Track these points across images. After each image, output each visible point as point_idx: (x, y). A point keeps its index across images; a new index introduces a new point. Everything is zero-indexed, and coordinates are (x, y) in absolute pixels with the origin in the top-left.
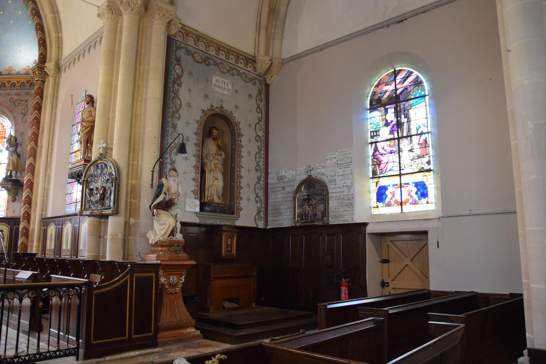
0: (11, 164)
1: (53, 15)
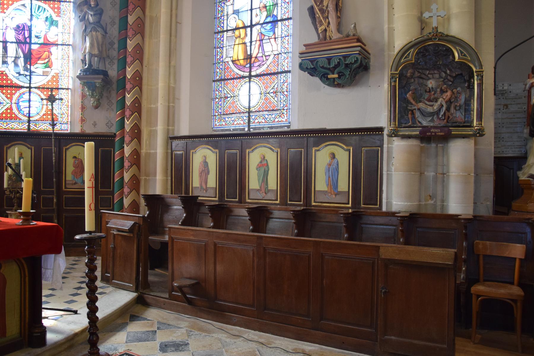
0: (96, 45)
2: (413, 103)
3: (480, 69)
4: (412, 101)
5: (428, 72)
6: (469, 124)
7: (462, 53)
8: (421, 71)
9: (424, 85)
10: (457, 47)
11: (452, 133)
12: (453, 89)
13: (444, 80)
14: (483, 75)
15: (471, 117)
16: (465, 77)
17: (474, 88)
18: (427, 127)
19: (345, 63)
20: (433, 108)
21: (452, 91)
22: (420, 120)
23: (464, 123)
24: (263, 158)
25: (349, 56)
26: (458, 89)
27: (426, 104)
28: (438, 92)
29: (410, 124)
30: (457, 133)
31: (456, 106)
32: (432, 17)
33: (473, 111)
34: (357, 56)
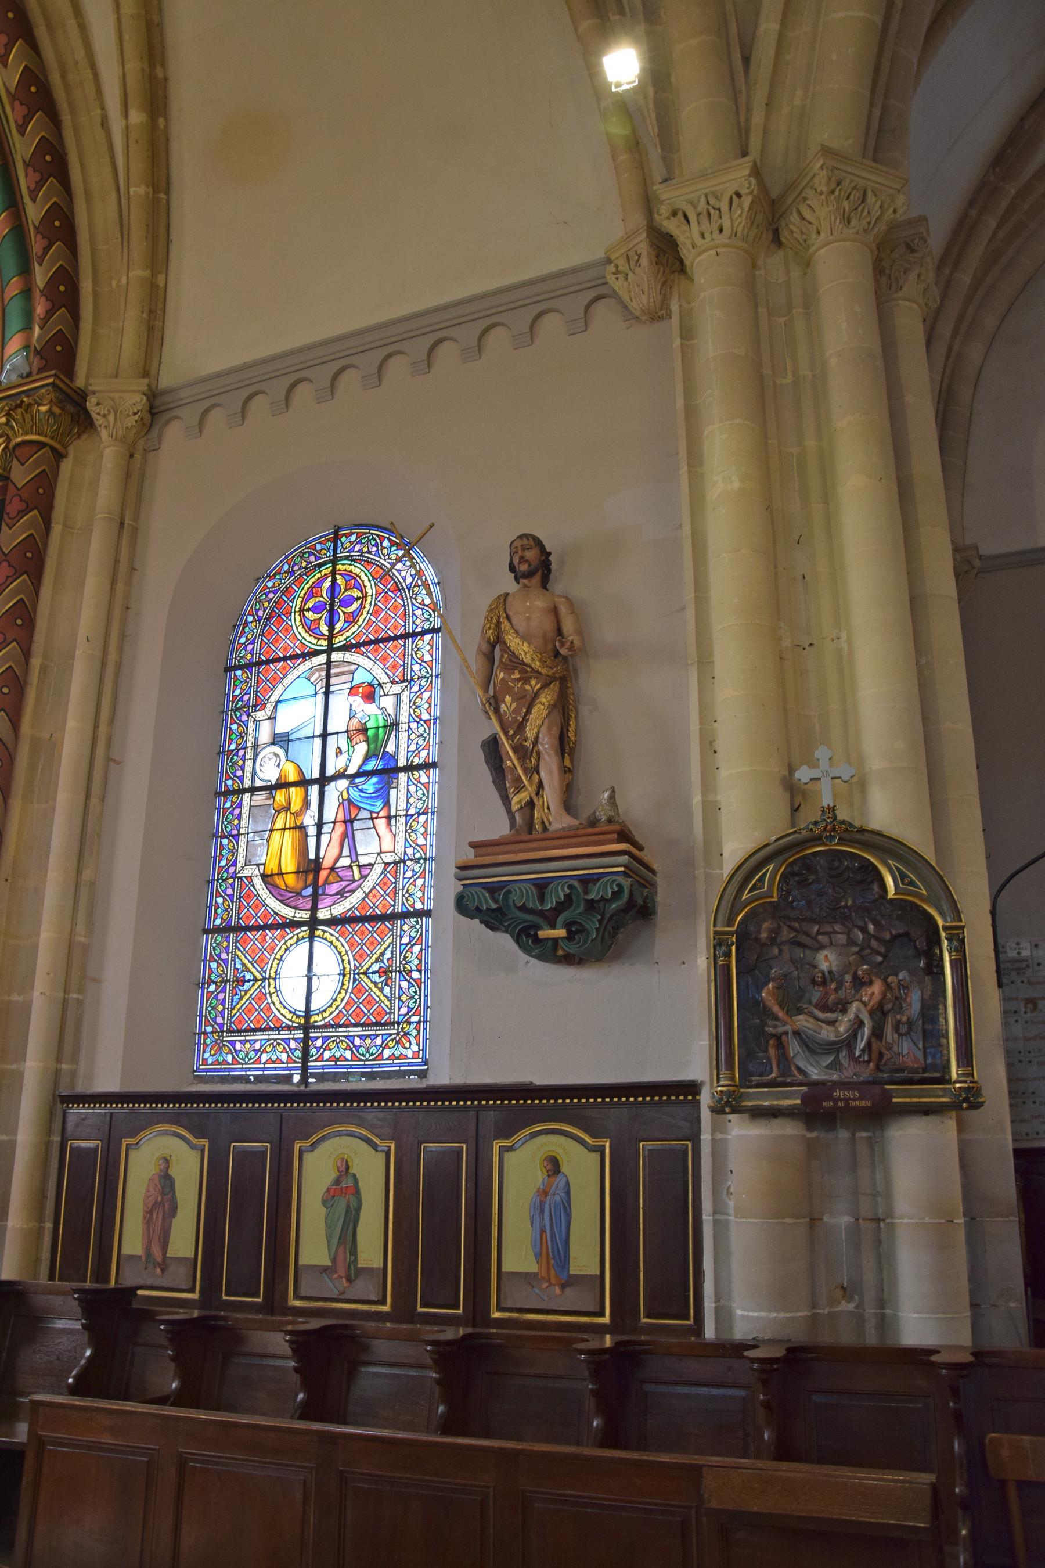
1: (151, 190)
2: (781, 1014)
3: (953, 920)
4: (776, 1009)
5: (816, 928)
6: (938, 1075)
7: (903, 876)
8: (797, 925)
9: (807, 963)
10: (890, 862)
11: (894, 1100)
12: (889, 976)
13: (860, 951)
14: (964, 938)
15: (942, 1055)
16: (917, 943)
17: (943, 973)
18: (822, 1083)
19: (586, 897)
20: (837, 1031)
21: (885, 980)
22: (801, 1064)
23: (925, 1071)
24: (345, 1170)
25: (598, 880)
26: (901, 977)
27: (817, 1019)
28: (848, 984)
29: (774, 1075)
30: (908, 1100)
31: (899, 1022)
32: (819, 779)
33: (947, 1038)
34: (620, 879)
